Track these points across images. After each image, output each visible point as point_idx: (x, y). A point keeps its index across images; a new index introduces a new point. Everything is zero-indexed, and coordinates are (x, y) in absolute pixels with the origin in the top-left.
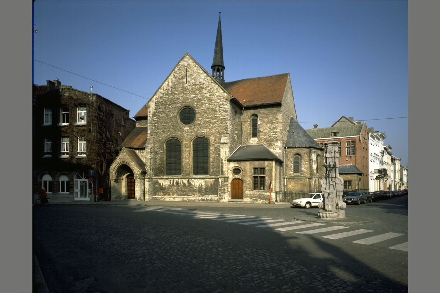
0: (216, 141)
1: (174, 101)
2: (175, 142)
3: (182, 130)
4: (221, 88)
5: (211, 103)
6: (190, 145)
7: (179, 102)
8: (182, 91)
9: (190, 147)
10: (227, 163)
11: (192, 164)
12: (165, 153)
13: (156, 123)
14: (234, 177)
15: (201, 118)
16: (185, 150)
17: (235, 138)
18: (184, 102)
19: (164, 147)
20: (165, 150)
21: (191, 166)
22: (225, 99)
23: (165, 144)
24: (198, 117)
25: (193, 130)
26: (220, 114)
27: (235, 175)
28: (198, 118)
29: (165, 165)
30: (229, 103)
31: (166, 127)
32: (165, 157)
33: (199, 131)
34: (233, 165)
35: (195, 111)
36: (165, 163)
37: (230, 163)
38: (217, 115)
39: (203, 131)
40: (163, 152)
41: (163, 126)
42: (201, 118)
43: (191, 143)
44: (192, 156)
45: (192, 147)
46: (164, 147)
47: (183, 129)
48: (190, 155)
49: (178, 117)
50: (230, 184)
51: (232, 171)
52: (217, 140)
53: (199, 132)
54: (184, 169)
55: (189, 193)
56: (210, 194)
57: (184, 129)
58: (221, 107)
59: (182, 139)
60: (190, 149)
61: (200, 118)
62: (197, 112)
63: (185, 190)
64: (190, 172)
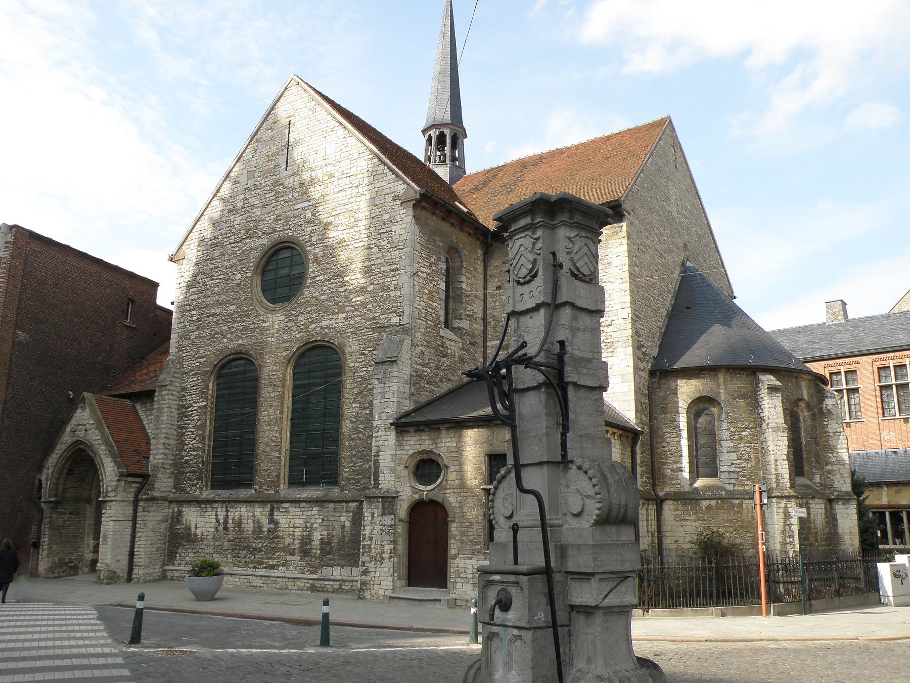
0: (364, 354)
1: (248, 230)
2: (243, 369)
3: (264, 324)
4: (389, 168)
5: (355, 221)
6: (284, 376)
7: (260, 234)
8: (273, 194)
9: (284, 386)
10: (392, 435)
11: (286, 445)
12: (212, 409)
13: (194, 309)
14: (417, 496)
15: (321, 278)
16: (268, 395)
17: (448, 343)
18: (275, 231)
19: (210, 387)
20: (212, 397)
21: (283, 453)
22: (399, 202)
23: (213, 377)
24: (313, 275)
25: (296, 322)
26: (379, 255)
27: (422, 487)
28: (312, 278)
29: (209, 451)
30: (411, 212)
31: (219, 320)
32: (210, 423)
33: (312, 322)
34: (415, 444)
35: (306, 252)
36: (209, 446)
37: (405, 439)
38: (372, 262)
39: (325, 323)
40: (205, 407)
41: (213, 315)
42: (321, 278)
43: (289, 370)
44: (290, 417)
45: (289, 383)
46: (210, 387)
47: (265, 322)
48: (281, 412)
49: (257, 281)
50: (401, 523)
51: (412, 468)
52: (370, 351)
53: (313, 326)
54: (264, 466)
55: (270, 558)
56: (338, 565)
57: (270, 320)
58: (384, 231)
59: (263, 358)
60: (284, 391)
61: (318, 279)
62: (311, 257)
63: (260, 545)
64: (278, 476)
